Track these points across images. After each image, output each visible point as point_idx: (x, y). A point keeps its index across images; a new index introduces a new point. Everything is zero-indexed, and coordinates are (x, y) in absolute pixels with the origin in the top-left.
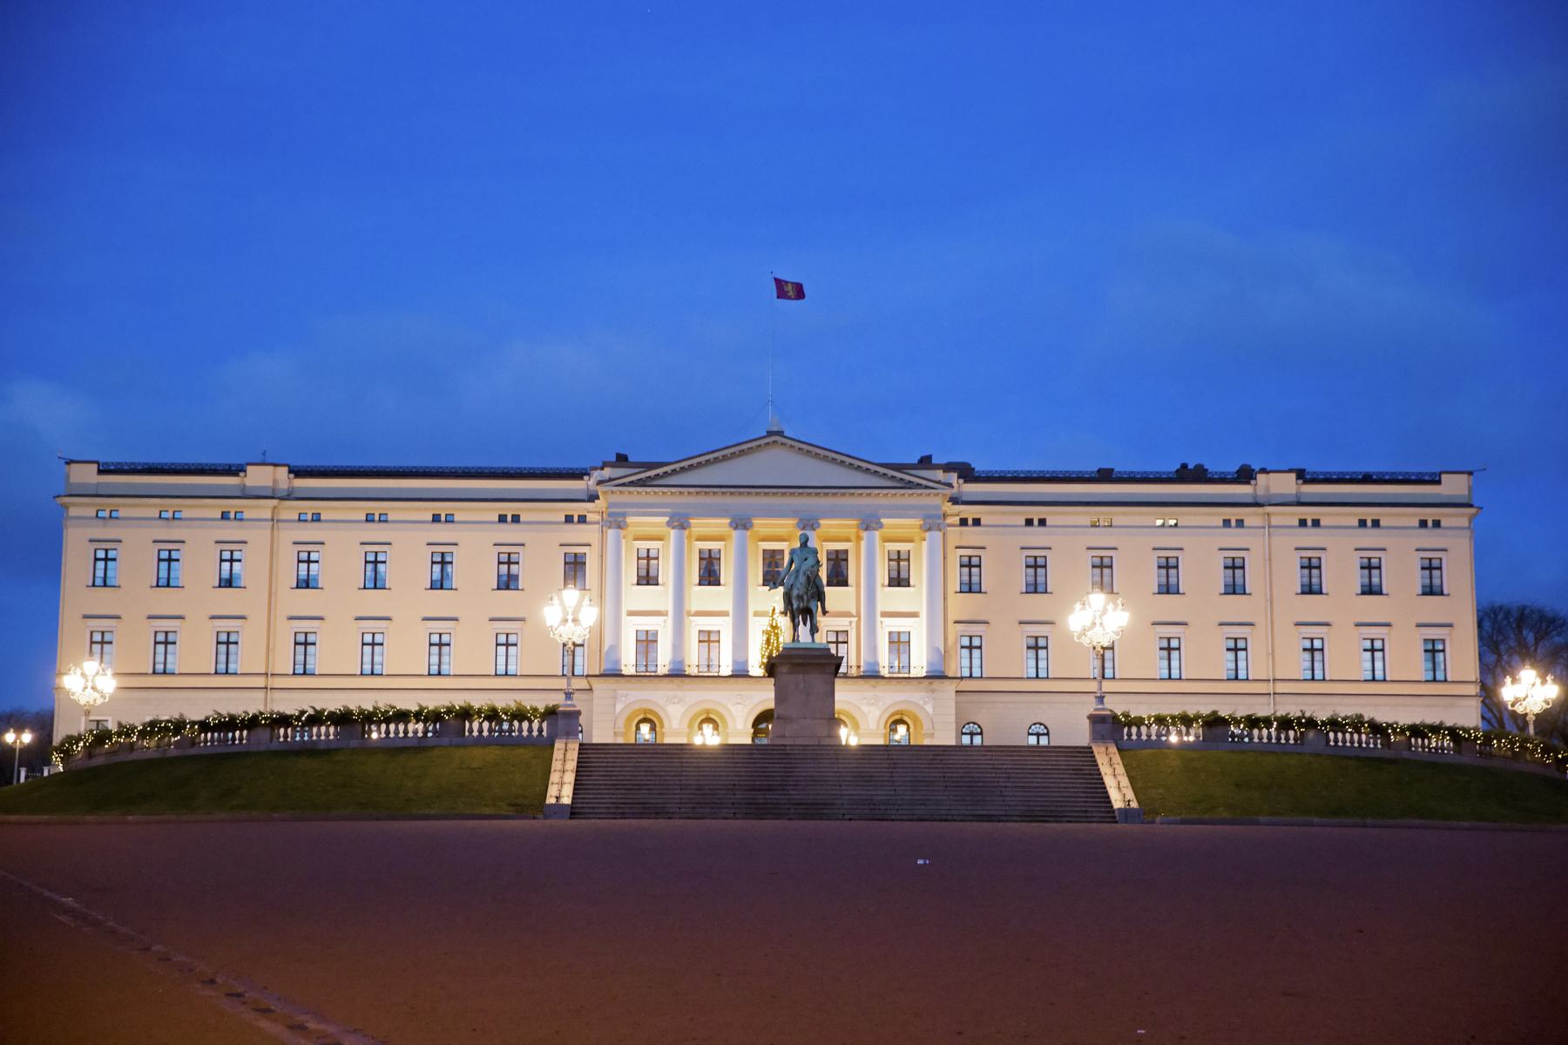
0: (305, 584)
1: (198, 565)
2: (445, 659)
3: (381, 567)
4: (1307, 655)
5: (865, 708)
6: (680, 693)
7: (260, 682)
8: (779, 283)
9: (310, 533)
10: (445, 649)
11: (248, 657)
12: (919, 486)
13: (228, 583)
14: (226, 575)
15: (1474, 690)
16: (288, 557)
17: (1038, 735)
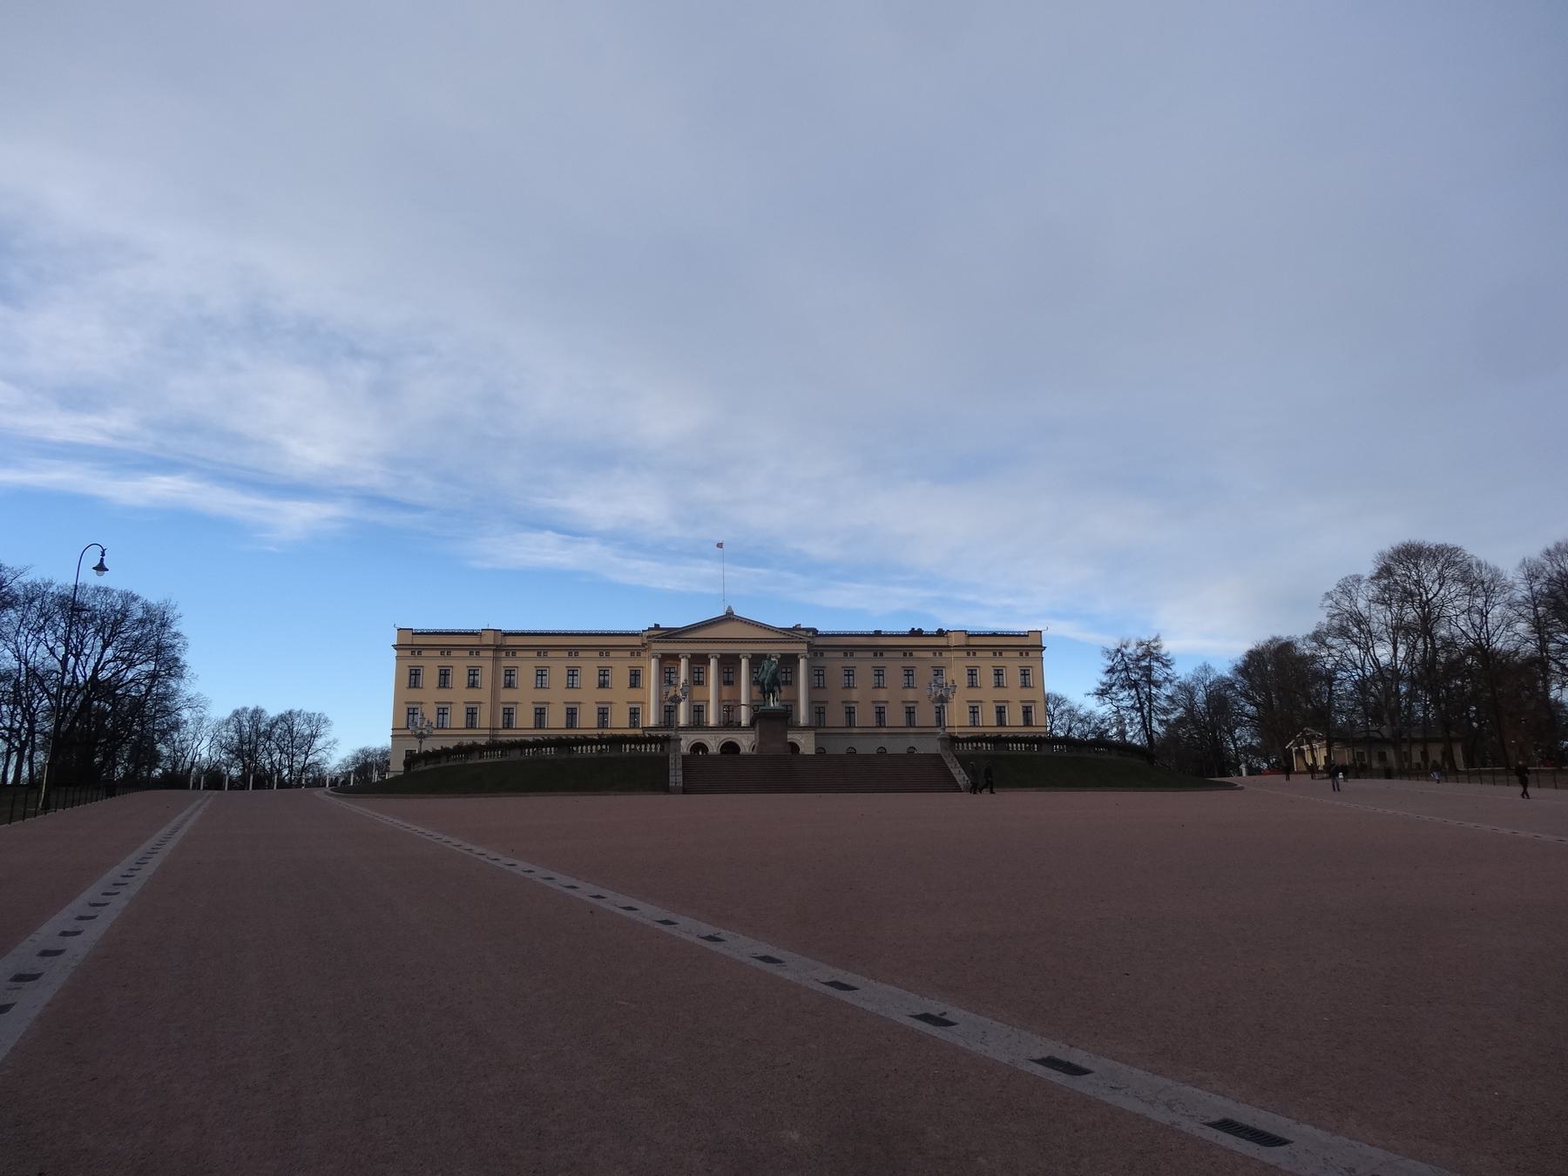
0: (509, 685)
1: (459, 677)
11: (484, 719)
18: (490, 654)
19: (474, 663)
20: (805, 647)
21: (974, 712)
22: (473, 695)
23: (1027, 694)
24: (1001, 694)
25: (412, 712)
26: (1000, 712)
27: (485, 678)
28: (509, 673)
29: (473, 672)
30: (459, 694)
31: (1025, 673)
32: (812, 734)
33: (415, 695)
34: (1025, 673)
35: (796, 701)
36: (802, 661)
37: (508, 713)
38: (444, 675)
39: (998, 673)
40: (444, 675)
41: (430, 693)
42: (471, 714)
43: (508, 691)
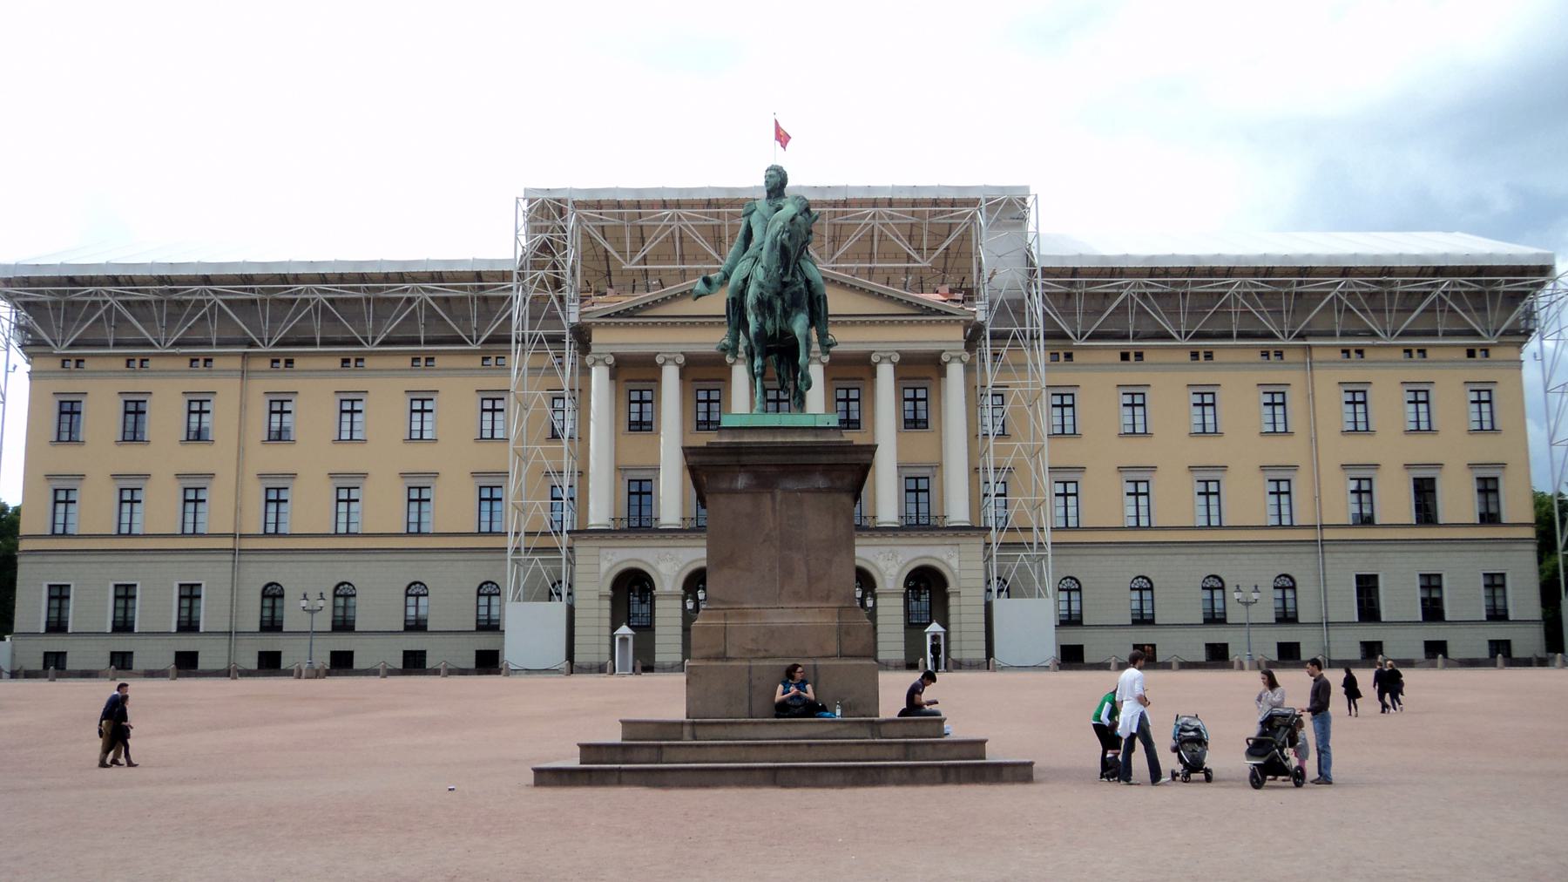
0: (279, 436)
1: (166, 415)
2: (424, 518)
3: (357, 417)
4: (1354, 497)
5: (881, 564)
6: (673, 551)
7: (228, 543)
8: (784, 146)
9: (281, 383)
10: (424, 505)
11: (216, 516)
12: (938, 312)
13: (198, 436)
14: (194, 426)
15: (1530, 533)
16: (260, 407)
17: (1069, 590)
18: (236, 363)
19: (200, 383)
20: (957, 334)
21: (1363, 491)
22: (196, 458)
23: (1486, 449)
24: (1423, 450)
25: (63, 498)
26: (1424, 491)
27: (219, 421)
28: (279, 406)
29: (198, 406)
30: (164, 454)
31: (1483, 396)
32: (974, 546)
33: (67, 459)
34: (1483, 396)
35: (939, 466)
36: (955, 372)
37: (275, 499)
38: (134, 410)
39: (1420, 396)
40: (134, 410)
41: (100, 451)
42: (193, 499)
43: (278, 449)
